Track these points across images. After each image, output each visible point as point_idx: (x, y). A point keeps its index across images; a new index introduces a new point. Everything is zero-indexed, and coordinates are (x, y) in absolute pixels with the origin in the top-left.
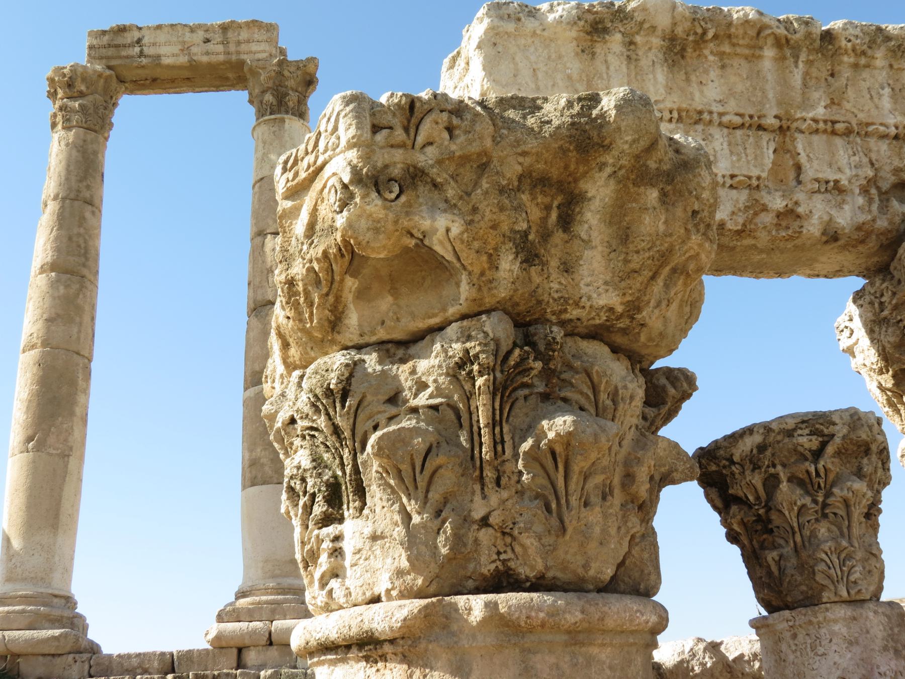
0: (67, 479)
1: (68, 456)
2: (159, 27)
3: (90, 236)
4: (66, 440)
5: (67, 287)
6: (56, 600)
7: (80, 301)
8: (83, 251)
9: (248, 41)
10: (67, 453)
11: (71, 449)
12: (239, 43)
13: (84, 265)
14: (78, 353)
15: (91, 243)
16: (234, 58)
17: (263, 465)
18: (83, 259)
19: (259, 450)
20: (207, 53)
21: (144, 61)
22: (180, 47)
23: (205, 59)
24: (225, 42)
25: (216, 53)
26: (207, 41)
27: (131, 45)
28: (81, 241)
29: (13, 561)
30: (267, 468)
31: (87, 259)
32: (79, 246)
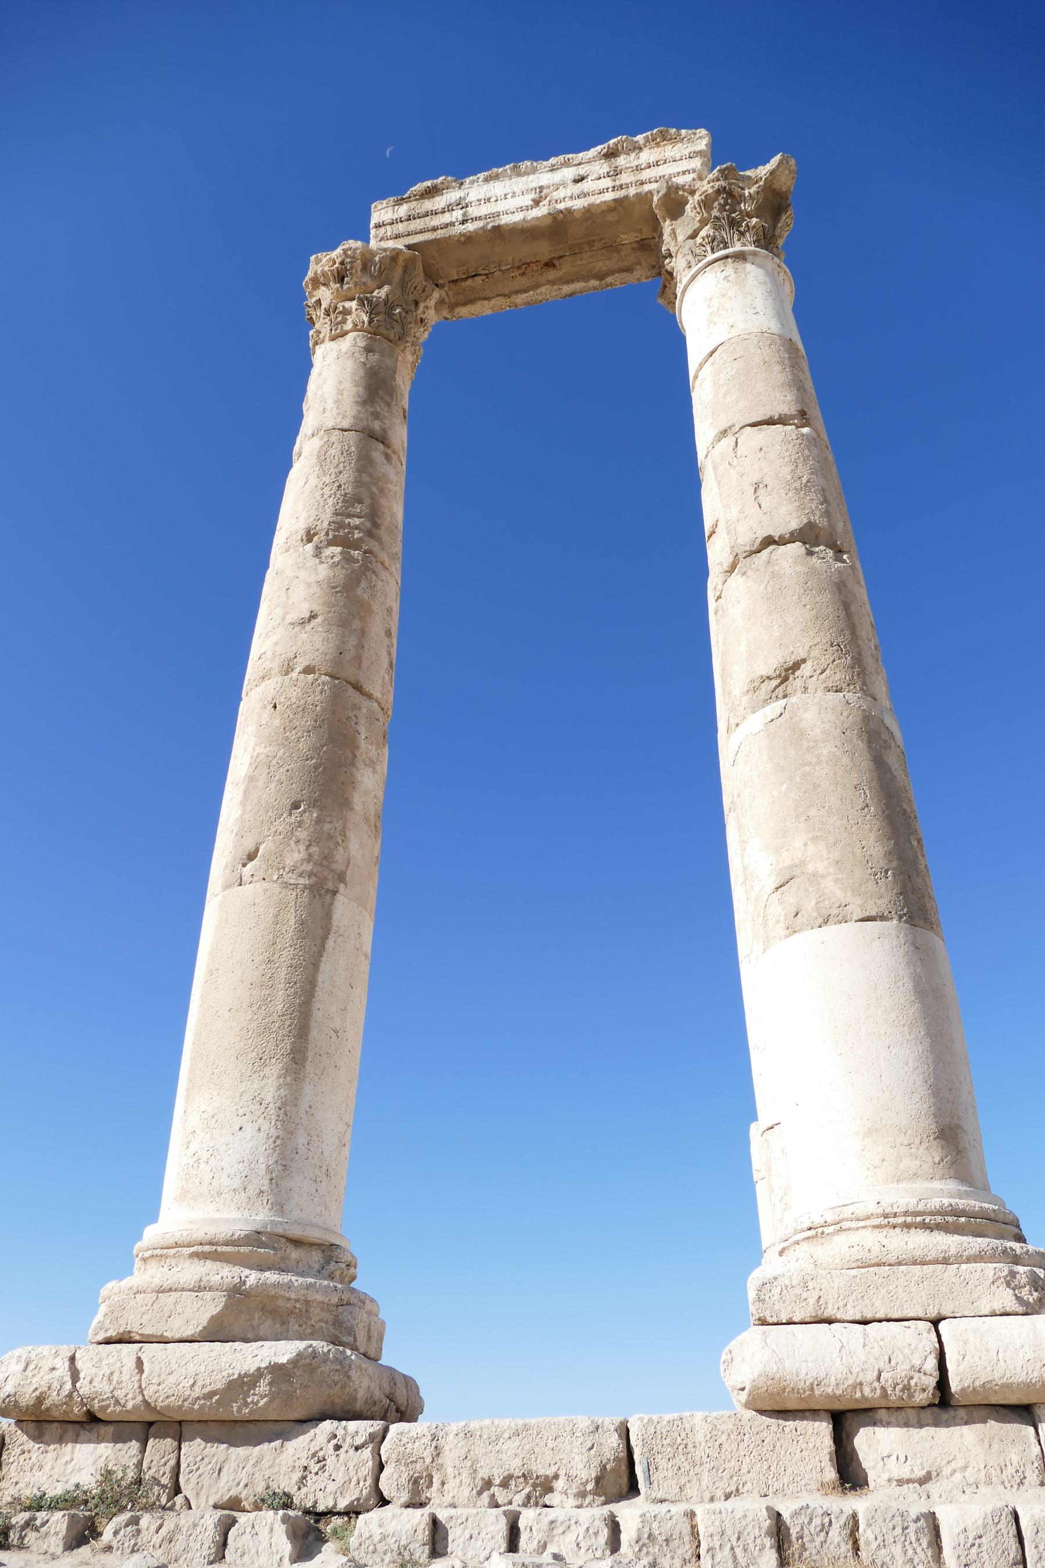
0: (330, 944)
1: (335, 893)
3: (382, 490)
6: (295, 1254)
10: (330, 885)
11: (341, 878)
12: (638, 169)
14: (358, 688)
15: (383, 501)
16: (632, 191)
17: (815, 878)
19: (798, 844)
20: (584, 195)
21: (471, 227)
22: (533, 196)
23: (578, 204)
26: (580, 179)
29: (193, 1147)
30: (829, 885)
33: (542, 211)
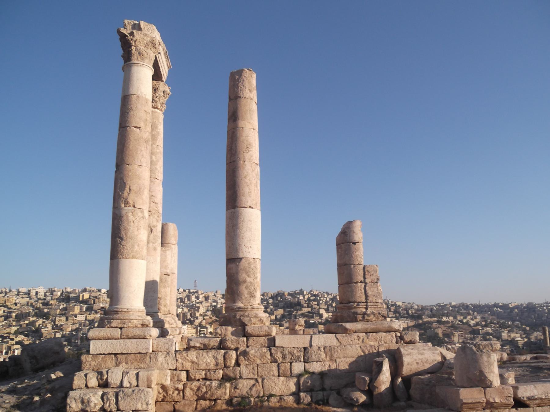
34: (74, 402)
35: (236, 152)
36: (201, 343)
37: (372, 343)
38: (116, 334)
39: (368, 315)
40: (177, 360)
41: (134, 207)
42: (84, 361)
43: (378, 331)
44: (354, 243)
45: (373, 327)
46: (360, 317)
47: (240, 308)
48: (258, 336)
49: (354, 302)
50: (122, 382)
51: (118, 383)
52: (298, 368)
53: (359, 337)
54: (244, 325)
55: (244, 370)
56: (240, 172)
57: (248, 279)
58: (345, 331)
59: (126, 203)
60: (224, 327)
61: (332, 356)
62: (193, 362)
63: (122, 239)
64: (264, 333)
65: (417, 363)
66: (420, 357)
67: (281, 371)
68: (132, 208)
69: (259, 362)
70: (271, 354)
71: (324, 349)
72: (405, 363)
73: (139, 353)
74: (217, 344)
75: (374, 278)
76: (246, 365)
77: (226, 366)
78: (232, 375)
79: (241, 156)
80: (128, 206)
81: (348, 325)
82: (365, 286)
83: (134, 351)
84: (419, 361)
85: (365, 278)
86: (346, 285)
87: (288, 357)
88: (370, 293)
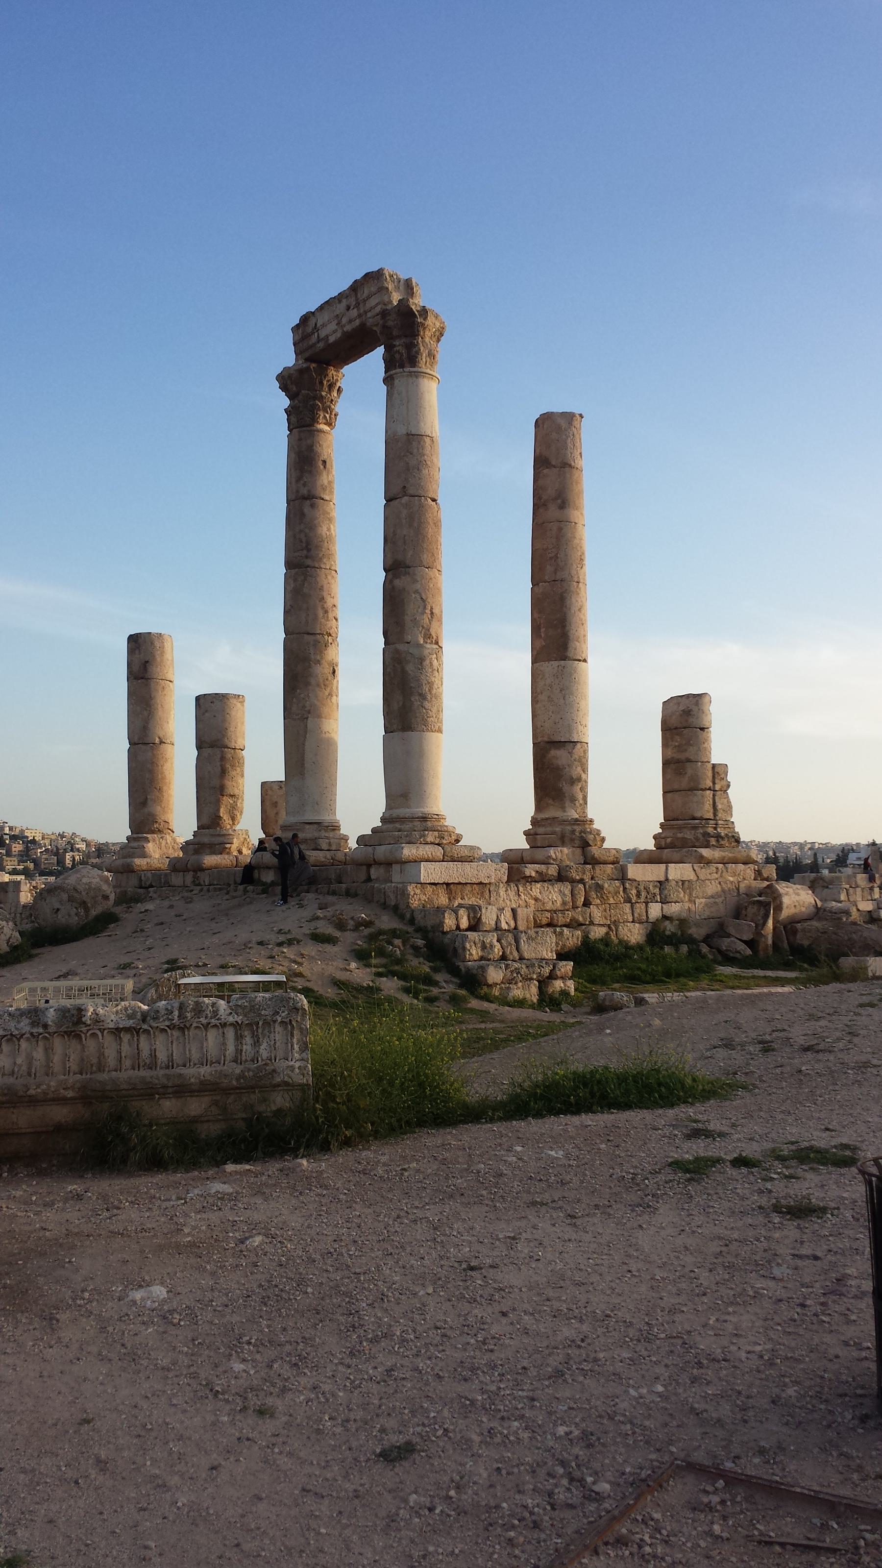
1: (307, 718)
2: (321, 308)
4: (304, 707)
5: (295, 580)
6: (307, 827)
7: (305, 590)
8: (304, 545)
9: (369, 297)
11: (309, 712)
13: (307, 557)
18: (305, 552)
20: (350, 321)
21: (321, 345)
22: (336, 322)
23: (348, 328)
24: (357, 306)
25: (351, 321)
27: (313, 333)
28: (302, 536)
31: (309, 550)
32: (301, 542)
33: (339, 334)
34: (473, 947)
35: (566, 564)
36: (537, 872)
37: (731, 879)
38: (439, 854)
39: (723, 838)
40: (519, 895)
41: (437, 643)
42: (412, 893)
43: (735, 862)
44: (702, 729)
45: (730, 855)
46: (713, 841)
47: (576, 820)
48: (605, 863)
49: (701, 819)
50: (498, 921)
51: (493, 923)
52: (655, 911)
53: (717, 868)
54: (585, 845)
55: (596, 913)
56: (573, 600)
57: (584, 776)
58: (701, 860)
59: (428, 636)
60: (559, 849)
61: (691, 894)
62: (536, 899)
63: (425, 698)
64: (611, 859)
65: (795, 906)
66: (797, 898)
67: (636, 915)
68: (436, 646)
69: (612, 901)
70: (625, 889)
71: (683, 884)
72: (785, 906)
73: (481, 883)
74: (556, 874)
75: (724, 783)
76: (597, 905)
77: (575, 907)
78: (581, 919)
79: (573, 573)
80: (429, 641)
81: (705, 852)
82: (714, 795)
83: (474, 881)
84: (797, 904)
85: (714, 783)
86: (689, 793)
87: (643, 894)
88: (719, 806)
